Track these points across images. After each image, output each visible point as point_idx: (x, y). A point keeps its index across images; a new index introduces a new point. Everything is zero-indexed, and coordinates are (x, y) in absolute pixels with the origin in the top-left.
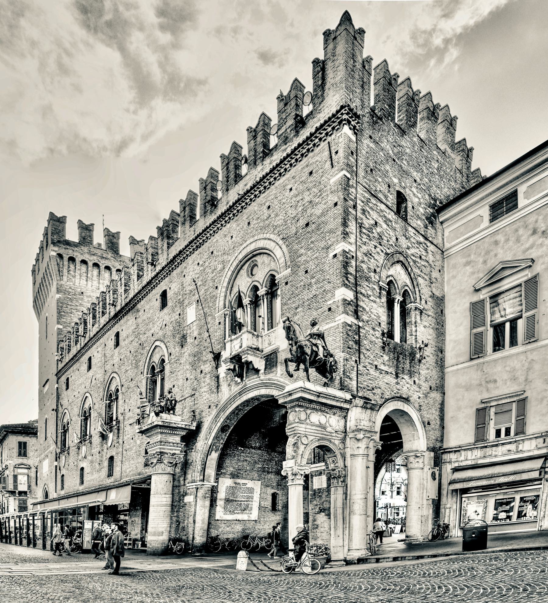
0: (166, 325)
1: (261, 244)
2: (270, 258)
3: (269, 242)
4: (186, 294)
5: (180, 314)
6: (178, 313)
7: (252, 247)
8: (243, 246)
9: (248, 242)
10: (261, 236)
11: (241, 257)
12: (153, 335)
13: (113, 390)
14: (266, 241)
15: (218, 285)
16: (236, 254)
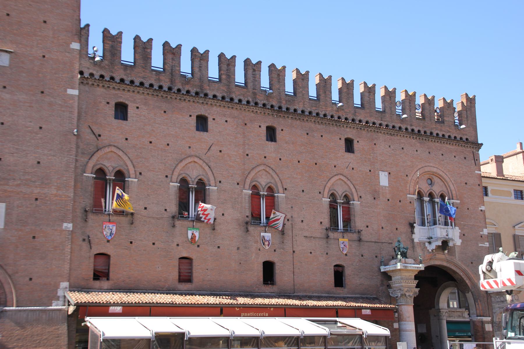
0: (353, 169)
1: (441, 173)
2: (442, 183)
4: (377, 159)
5: (370, 171)
6: (369, 168)
7: (435, 170)
9: (431, 165)
12: (335, 166)
13: (264, 184)
14: (444, 174)
15: (408, 175)
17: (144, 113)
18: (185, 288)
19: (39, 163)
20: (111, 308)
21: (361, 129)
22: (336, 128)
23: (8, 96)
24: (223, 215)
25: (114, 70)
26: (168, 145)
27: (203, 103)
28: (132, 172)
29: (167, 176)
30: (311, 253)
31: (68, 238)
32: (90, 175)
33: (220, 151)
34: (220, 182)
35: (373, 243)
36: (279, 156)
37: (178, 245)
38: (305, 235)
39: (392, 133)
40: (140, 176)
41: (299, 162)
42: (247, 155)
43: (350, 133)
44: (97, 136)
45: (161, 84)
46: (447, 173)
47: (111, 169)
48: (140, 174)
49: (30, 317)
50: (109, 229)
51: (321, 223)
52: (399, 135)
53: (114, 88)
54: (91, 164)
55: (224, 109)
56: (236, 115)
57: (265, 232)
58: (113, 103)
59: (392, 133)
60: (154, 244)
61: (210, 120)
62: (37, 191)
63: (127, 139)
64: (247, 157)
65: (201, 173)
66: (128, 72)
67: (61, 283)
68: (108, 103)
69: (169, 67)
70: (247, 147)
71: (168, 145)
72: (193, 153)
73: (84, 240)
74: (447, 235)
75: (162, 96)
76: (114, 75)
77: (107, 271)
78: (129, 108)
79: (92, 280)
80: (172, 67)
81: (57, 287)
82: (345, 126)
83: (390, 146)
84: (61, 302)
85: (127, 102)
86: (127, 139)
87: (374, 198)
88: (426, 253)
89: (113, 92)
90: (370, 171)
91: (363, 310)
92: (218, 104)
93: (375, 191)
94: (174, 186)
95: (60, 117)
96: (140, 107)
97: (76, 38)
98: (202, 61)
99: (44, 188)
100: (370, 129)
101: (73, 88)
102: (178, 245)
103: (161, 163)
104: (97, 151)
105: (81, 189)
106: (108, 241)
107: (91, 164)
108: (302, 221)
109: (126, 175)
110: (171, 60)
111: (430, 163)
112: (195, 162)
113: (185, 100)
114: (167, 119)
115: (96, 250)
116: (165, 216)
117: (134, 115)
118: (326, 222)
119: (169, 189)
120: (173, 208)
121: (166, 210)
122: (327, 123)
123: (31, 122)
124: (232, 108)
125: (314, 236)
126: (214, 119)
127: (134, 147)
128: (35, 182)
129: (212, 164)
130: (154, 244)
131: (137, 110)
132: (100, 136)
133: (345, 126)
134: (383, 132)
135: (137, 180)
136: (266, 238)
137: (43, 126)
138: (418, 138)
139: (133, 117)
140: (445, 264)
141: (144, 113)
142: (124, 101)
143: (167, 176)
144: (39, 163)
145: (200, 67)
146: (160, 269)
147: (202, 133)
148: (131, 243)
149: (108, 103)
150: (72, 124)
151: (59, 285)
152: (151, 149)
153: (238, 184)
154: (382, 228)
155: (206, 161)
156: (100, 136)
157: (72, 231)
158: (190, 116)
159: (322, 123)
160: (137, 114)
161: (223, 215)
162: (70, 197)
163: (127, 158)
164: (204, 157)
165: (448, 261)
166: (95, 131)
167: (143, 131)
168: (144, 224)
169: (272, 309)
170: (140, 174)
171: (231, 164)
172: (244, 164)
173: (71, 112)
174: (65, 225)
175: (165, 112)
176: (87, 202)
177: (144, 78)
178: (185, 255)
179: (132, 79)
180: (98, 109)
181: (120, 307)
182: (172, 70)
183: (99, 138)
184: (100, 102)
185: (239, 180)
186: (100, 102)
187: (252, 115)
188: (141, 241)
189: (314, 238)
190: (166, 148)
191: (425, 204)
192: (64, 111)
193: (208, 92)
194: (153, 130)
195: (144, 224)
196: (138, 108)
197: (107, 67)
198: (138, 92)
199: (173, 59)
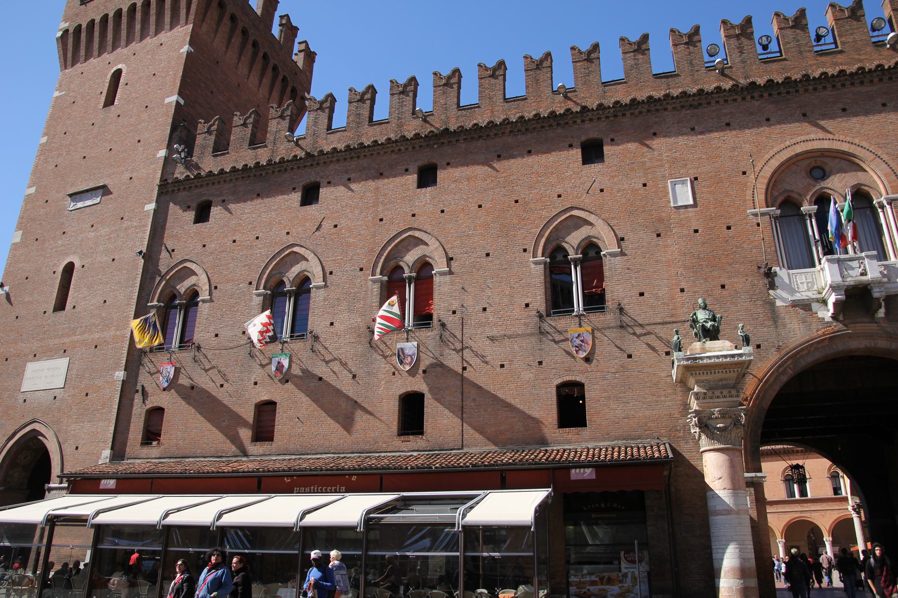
0: (602, 190)
3: (859, 148)
4: (661, 160)
7: (826, 145)
8: (803, 138)
10: (841, 138)
11: (799, 149)
14: (853, 147)
16: (788, 143)
18: (261, 452)
20: (103, 482)
21: (615, 116)
22: (560, 130)
23: (93, 234)
24: (332, 324)
27: (312, 165)
30: (502, 366)
33: (336, 226)
34: (331, 273)
35: (659, 326)
36: (441, 207)
37: (256, 383)
38: (490, 334)
39: (696, 103)
41: (480, 206)
42: (381, 220)
43: (592, 132)
46: (864, 144)
51: (527, 305)
52: (713, 102)
53: (196, 186)
55: (347, 164)
56: (365, 165)
57: (408, 340)
59: (696, 103)
64: (381, 223)
70: (380, 208)
74: (864, 274)
75: (255, 176)
82: (579, 121)
83: (693, 129)
87: (659, 235)
88: (814, 326)
89: (197, 191)
90: (645, 185)
91: (573, 471)
92: (334, 159)
93: (660, 220)
100: (637, 112)
102: (256, 383)
108: (485, 309)
111: (808, 134)
113: (286, 170)
115: (149, 405)
118: (539, 300)
122: (539, 126)
124: (358, 157)
125: (508, 333)
129: (319, 251)
132: (173, 250)
133: (579, 121)
134: (669, 107)
136: (407, 352)
138: (766, 95)
140: (882, 344)
146: (225, 424)
147: (308, 208)
153: (361, 269)
154: (682, 290)
159: (527, 130)
161: (332, 324)
165: (890, 337)
169: (354, 478)
171: (352, 240)
172: (374, 236)
174: (117, 373)
178: (265, 398)
181: (114, 480)
183: (173, 254)
185: (364, 263)
187: (394, 156)
189: (510, 337)
191: (808, 221)
198: (225, 181)
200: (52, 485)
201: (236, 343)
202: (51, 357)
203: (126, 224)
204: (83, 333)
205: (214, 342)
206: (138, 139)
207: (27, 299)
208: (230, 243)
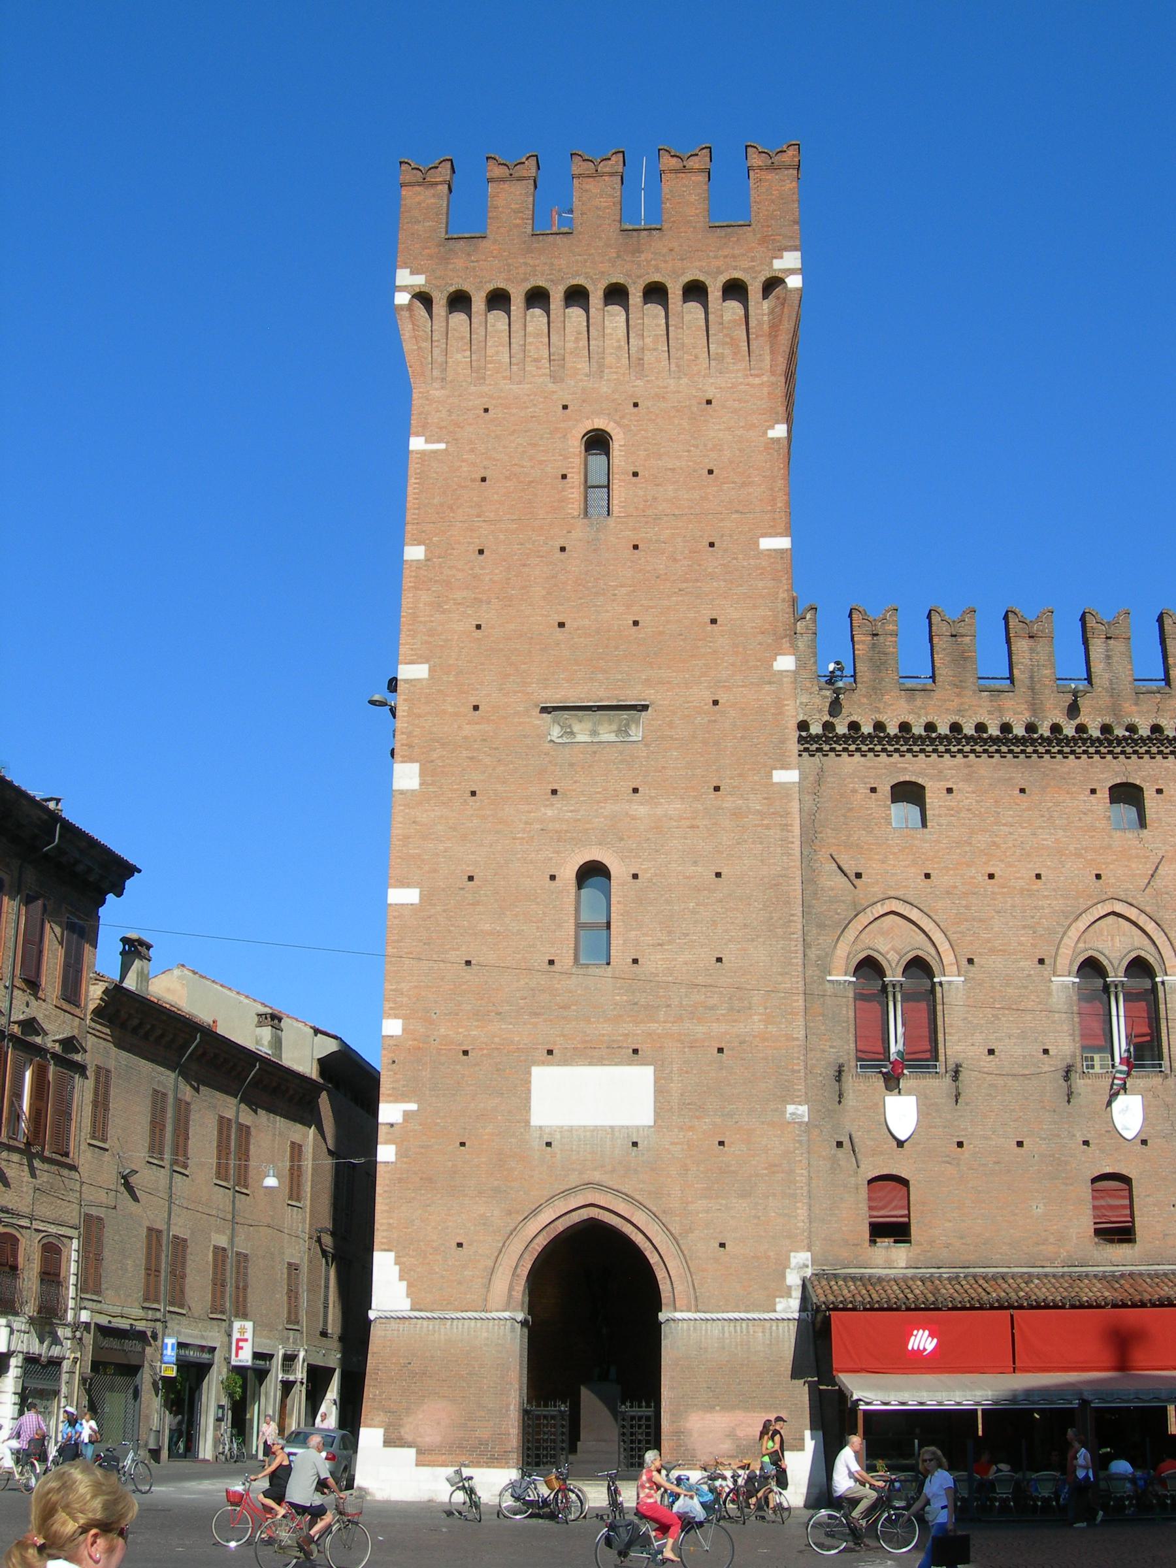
17: (967, 802)
19: (719, 960)
23: (641, 810)
25: (881, 705)
26: (1038, 876)
28: (949, 958)
29: (1041, 961)
31: (800, 1142)
32: (841, 975)
40: (970, 967)
44: (853, 877)
45: (1006, 719)
47: (893, 957)
48: (970, 961)
49: (727, 1335)
50: (902, 1112)
54: (842, 950)
58: (885, 789)
60: (1020, 1144)
61: (1149, 794)
62: (718, 1028)
63: (927, 876)
65: (1137, 944)
66: (918, 703)
67: (792, 1254)
68: (873, 790)
69: (1023, 672)
71: (1038, 876)
72: (1111, 892)
73: (840, 1144)
76: (883, 718)
77: (906, 1219)
78: (928, 794)
79: (867, 1243)
80: (1032, 671)
81: (784, 1265)
84: (795, 1303)
85: (920, 781)
86: (927, 876)
94: (1065, 986)
95: (761, 843)
96: (954, 787)
97: (786, 643)
98: (1111, 642)
99: (735, 1021)
101: (785, 767)
103: (1024, 927)
104: (856, 916)
105: (823, 1015)
106: (900, 1144)
107: (842, 950)
109: (936, 968)
110: (1027, 655)
112: (1114, 913)
114: (1028, 809)
116: (1046, 1068)
117: (944, 811)
119: (1050, 994)
120: (1065, 1045)
121: (1046, 1052)
123: (695, 863)
126: (1159, 791)
127: (948, 893)
128: (712, 1008)
130: (1020, 1144)
131: (950, 797)
135: (962, 979)
137: (724, 871)
139: (940, 816)
141: (967, 802)
142: (913, 779)
143: (1041, 961)
144: (719, 960)
145: (1108, 657)
148: (960, 1144)
149: (873, 790)
150: (791, 855)
151: (788, 1258)
152: (993, 893)
155: (1148, 909)
156: (859, 875)
157: (807, 1124)
158: (1093, 791)
160: (950, 809)
162: (797, 1039)
163: (932, 925)
164: (1140, 900)
166: (845, 868)
167: (967, 849)
168: (990, 1095)
170: (970, 961)
173: (786, 827)
174: (791, 1108)
175: (1022, 791)
176: (842, 1045)
177: (959, 712)
179: (930, 719)
180: (850, 810)
182: (1032, 677)
183: (857, 882)
184: (854, 791)
186: (854, 791)
188: (987, 1138)
190: (1035, 887)
192: (768, 827)
193: (1136, 720)
194: (994, 843)
195: (990, 1095)
196: (950, 791)
197: (865, 700)
199: (1032, 650)
200: (678, 1315)
201: (1033, 1070)
202: (601, 1061)
203: (729, 802)
204: (679, 1019)
205: (988, 1062)
206: (708, 615)
207: (487, 927)
208: (982, 879)
